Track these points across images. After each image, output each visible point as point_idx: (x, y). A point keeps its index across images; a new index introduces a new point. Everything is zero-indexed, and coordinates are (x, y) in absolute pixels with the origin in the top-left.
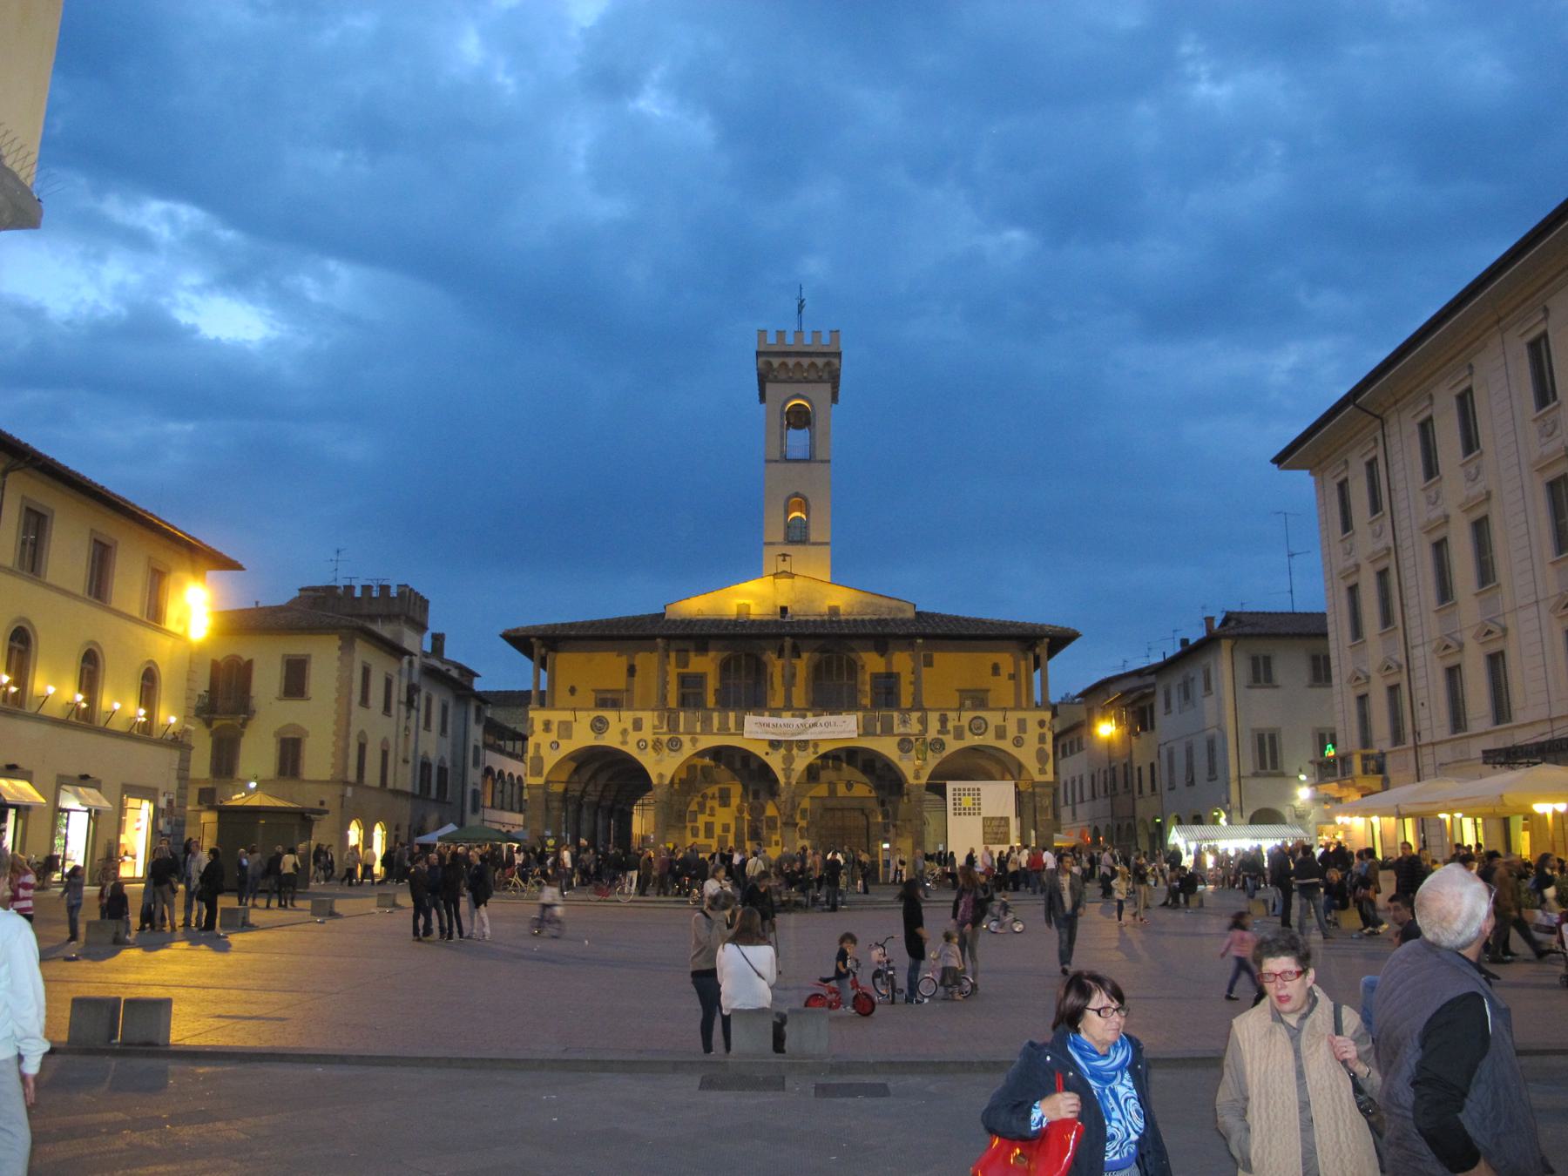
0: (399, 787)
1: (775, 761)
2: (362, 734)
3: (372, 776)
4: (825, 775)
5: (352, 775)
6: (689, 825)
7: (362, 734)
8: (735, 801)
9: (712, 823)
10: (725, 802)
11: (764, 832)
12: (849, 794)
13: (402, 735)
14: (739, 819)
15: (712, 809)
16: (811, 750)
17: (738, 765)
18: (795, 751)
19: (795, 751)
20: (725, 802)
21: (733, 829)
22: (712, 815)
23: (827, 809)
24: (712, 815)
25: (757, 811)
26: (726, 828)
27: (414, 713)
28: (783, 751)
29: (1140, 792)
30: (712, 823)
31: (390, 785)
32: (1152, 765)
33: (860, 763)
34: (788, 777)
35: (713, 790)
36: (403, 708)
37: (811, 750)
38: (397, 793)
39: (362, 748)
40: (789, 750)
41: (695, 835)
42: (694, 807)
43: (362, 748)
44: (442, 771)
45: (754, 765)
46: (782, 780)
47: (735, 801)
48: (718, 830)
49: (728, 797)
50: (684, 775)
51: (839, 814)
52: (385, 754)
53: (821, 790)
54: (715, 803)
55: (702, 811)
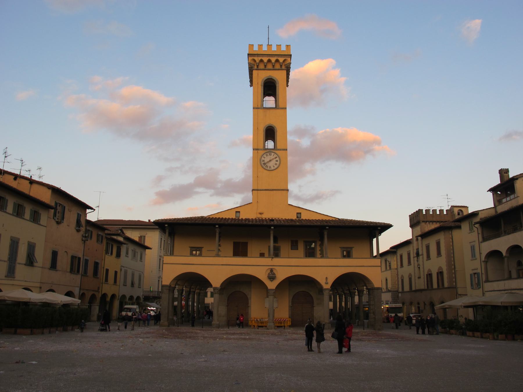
0: (417, 288)
2: (402, 276)
3: (407, 288)
5: (400, 290)
7: (402, 276)
13: (417, 269)
27: (421, 257)
29: (106, 280)
31: (413, 289)
32: (116, 273)
36: (416, 259)
38: (416, 291)
39: (402, 281)
43: (402, 281)
44: (440, 274)
52: (410, 279)
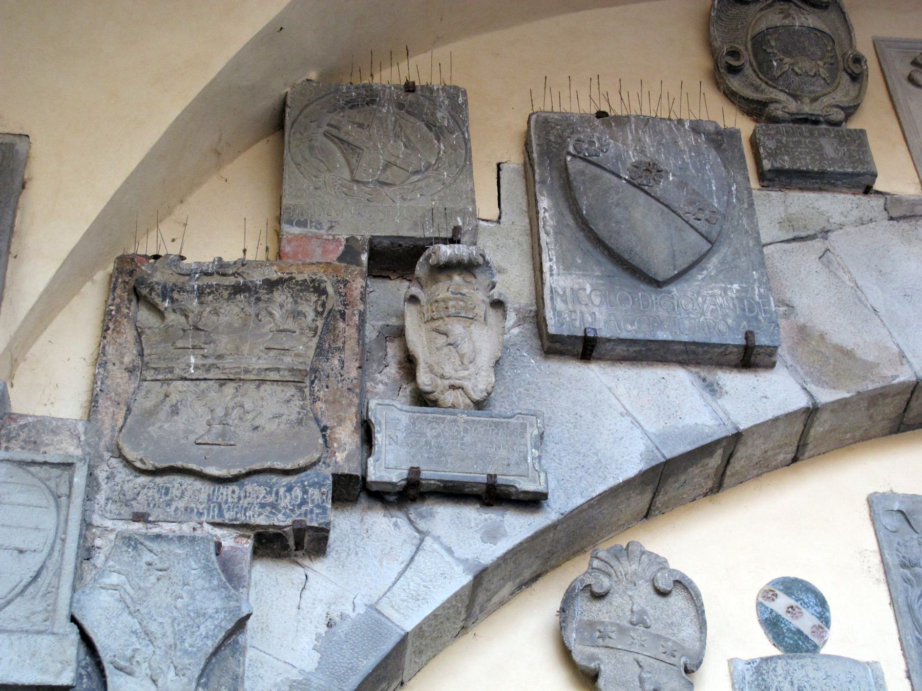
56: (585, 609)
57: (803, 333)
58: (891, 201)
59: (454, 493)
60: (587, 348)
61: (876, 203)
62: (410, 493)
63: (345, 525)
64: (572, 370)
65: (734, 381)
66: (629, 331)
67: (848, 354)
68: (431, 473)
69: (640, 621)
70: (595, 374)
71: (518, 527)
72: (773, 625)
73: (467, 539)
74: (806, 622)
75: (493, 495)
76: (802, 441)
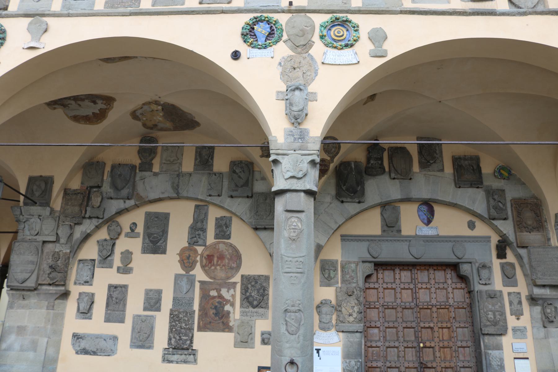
1: (259, 78)
4: (379, 188)
6: (75, 290)
8: (177, 237)
9: (124, 288)
10: (155, 243)
11: (236, 313)
12: (427, 231)
14: (183, 281)
15: (127, 256)
16: (364, 46)
17: (188, 164)
18: (318, 49)
19: (318, 49)
20: (155, 243)
21: (167, 303)
22: (125, 269)
23: (380, 265)
24: (125, 269)
25: (223, 260)
26: (153, 301)
28: (282, 50)
30: (124, 288)
33: (449, 169)
34: (297, 118)
35: (138, 217)
37: (364, 46)
40: (302, 46)
41: (85, 312)
42: (90, 251)
45: (221, 164)
46: (277, 127)
47: (177, 237)
48: (135, 305)
49: (165, 232)
50: (75, 185)
51: (405, 275)
53: (371, 224)
54: (134, 245)
55: (106, 259)
56: (110, 228)
57: (138, 194)
58: (154, 173)
59: (95, 218)
60: (111, 198)
61: (152, 173)
62: (90, 218)
63: (84, 220)
64: (111, 200)
65: (127, 201)
66: (115, 197)
67: (141, 197)
68: (91, 216)
69: (114, 229)
70: (113, 201)
71: (101, 221)
72: (131, 228)
73: (95, 222)
74: (134, 228)
75: (98, 218)
76: (137, 206)
